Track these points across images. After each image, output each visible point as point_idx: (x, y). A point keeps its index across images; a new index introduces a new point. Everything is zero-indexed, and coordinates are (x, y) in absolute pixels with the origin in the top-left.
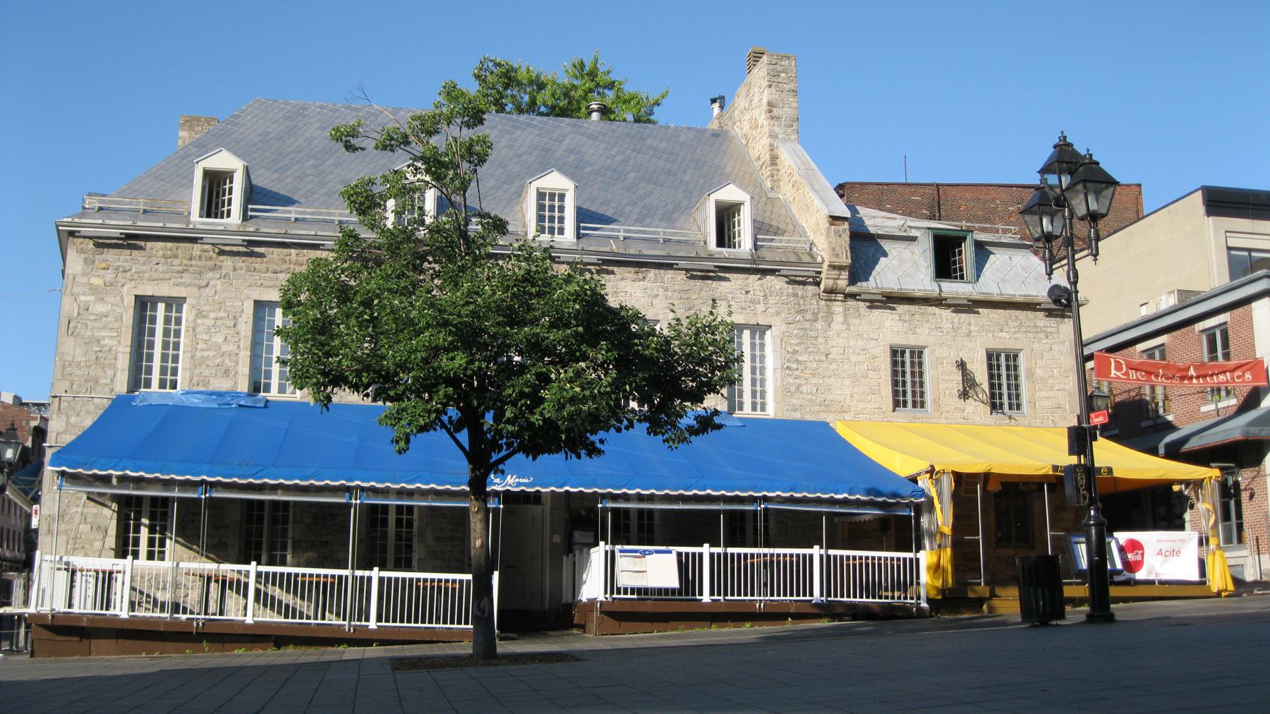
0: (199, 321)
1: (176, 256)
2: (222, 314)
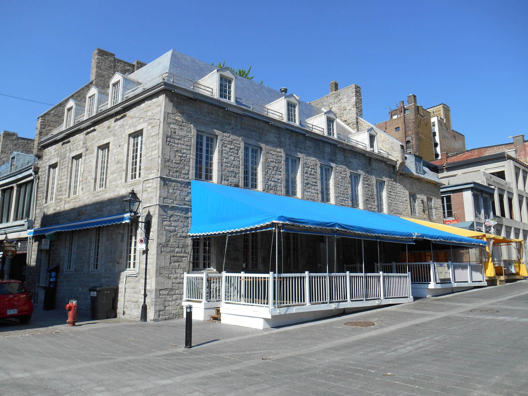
0: (223, 148)
1: (212, 114)
2: (232, 147)
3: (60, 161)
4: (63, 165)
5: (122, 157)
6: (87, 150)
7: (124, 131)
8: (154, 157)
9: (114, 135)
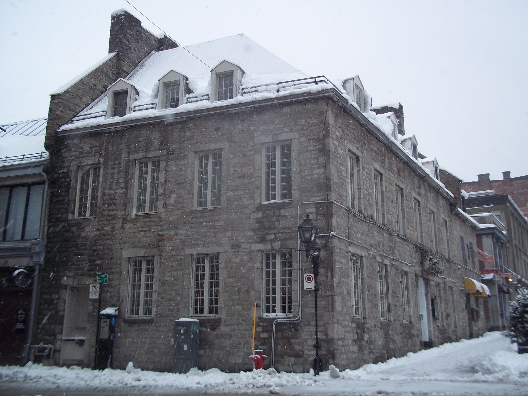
3: (106, 162)
4: (113, 168)
6: (170, 153)
7: (252, 138)
8: (317, 176)
9: (230, 140)
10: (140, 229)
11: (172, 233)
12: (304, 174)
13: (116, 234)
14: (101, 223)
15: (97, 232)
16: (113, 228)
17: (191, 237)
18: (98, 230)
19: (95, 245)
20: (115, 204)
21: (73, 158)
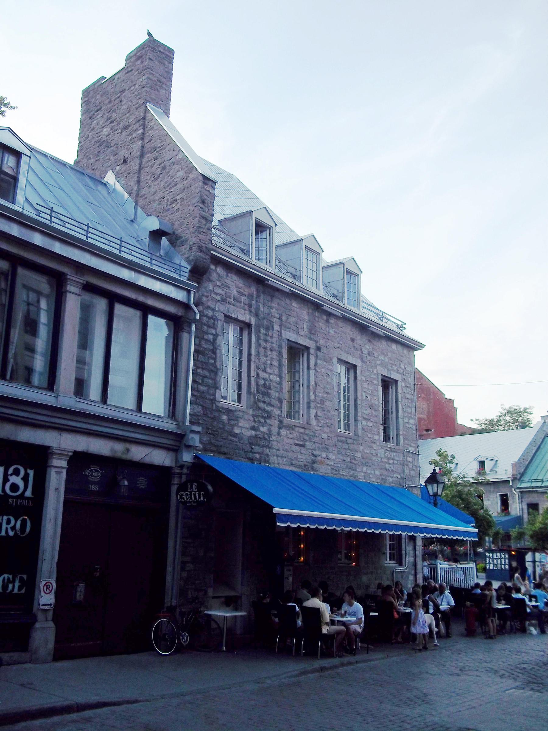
5: (377, 403)
10: (297, 442)
11: (324, 455)
12: (405, 421)
13: (273, 441)
14: (256, 420)
15: (253, 433)
16: (270, 430)
17: (339, 465)
18: (253, 428)
19: (251, 452)
20: (268, 395)
21: (218, 298)
